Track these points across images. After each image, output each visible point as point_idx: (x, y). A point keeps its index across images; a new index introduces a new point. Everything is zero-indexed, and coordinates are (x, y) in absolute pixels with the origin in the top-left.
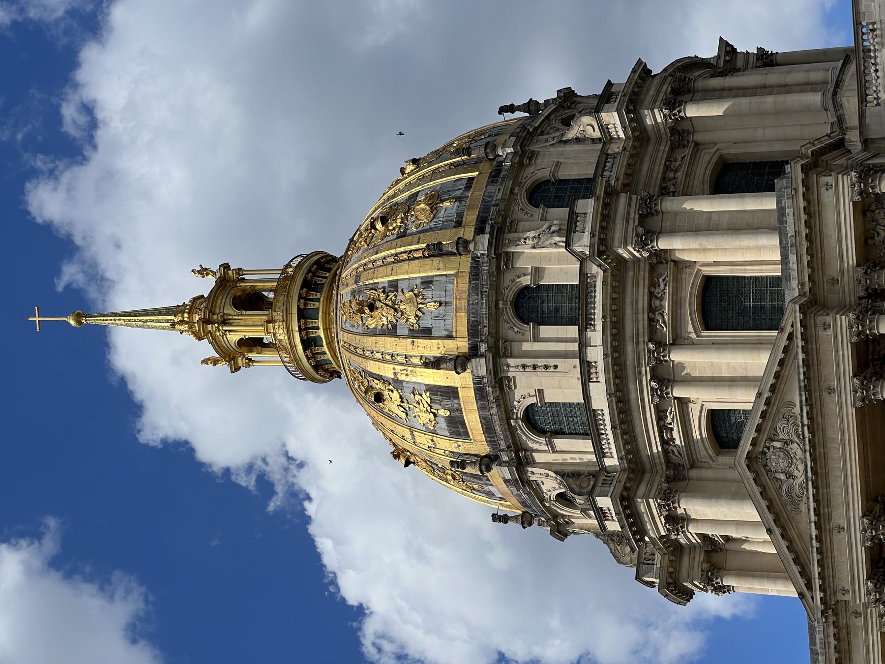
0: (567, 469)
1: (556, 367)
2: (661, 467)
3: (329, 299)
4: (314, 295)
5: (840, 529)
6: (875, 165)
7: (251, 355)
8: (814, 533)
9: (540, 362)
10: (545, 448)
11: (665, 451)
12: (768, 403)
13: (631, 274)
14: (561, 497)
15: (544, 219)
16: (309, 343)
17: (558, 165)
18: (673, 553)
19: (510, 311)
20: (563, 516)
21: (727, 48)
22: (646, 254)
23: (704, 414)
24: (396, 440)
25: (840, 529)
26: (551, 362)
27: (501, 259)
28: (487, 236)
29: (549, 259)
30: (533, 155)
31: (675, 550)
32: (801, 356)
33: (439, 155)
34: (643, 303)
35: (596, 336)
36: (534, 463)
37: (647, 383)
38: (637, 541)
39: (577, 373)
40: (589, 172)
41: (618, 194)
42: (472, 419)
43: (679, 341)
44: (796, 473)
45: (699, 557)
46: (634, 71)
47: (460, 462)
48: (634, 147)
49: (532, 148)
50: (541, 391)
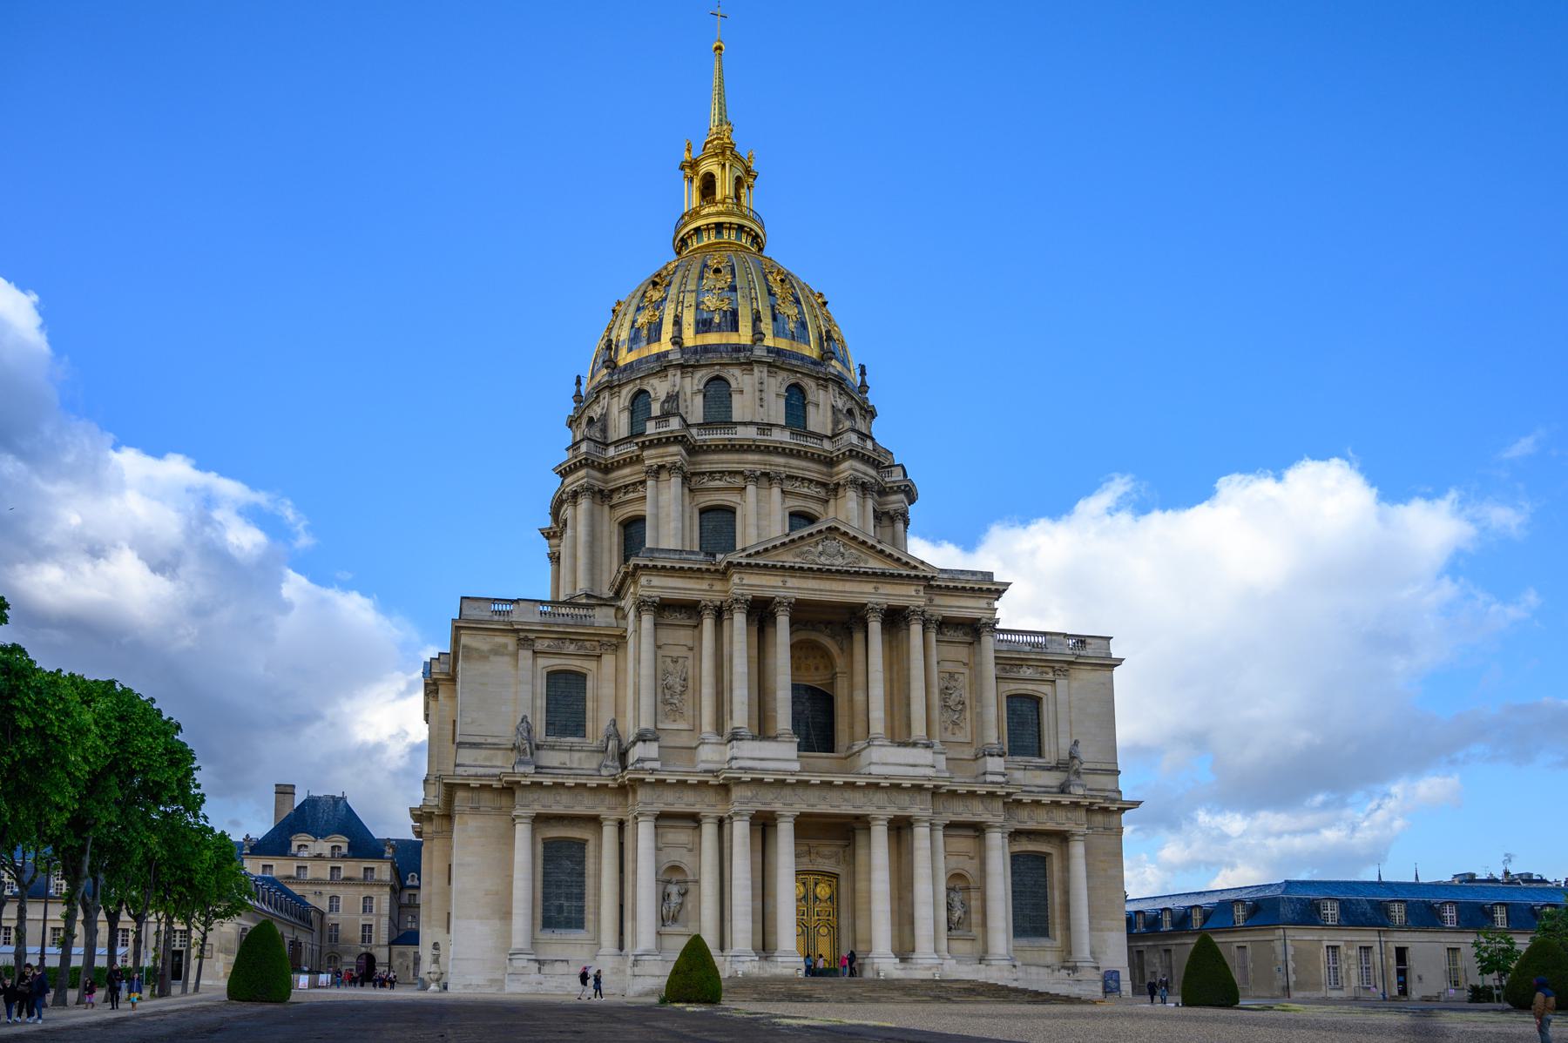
2: (692, 469)
5: (784, 582)
7: (696, 182)
13: (825, 470)
14: (642, 392)
16: (719, 227)
24: (677, 280)
25: (784, 582)
27: (825, 381)
34: (808, 475)
37: (760, 469)
42: (712, 339)
47: (677, 322)
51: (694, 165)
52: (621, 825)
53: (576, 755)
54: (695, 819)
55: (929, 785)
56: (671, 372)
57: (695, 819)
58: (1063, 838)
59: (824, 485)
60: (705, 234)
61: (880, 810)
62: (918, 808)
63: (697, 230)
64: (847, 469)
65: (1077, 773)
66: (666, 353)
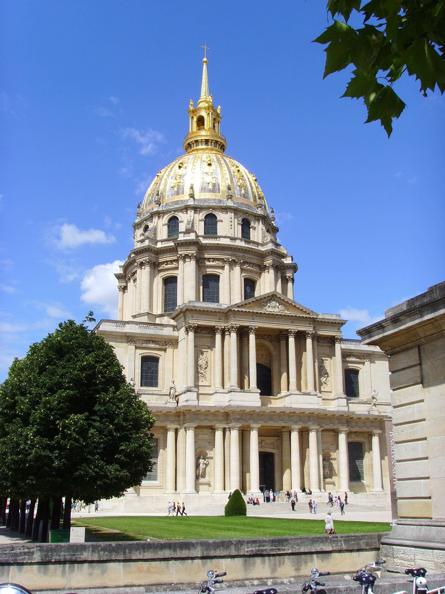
1: (231, 228)
4: (220, 147)
8: (255, 311)
9: (233, 224)
10: (201, 218)
16: (207, 142)
18: (157, 252)
19: (245, 217)
20: (163, 216)
22: (267, 265)
23: (218, 274)
26: (233, 227)
27: (258, 218)
29: (258, 232)
32: (305, 316)
36: (195, 213)
38: (178, 244)
43: (242, 270)
44: (270, 309)
45: (154, 260)
47: (192, 188)
50: (222, 221)
52: (176, 431)
53: (155, 397)
54: (213, 429)
63: (197, 141)
65: (375, 405)
66: (187, 201)
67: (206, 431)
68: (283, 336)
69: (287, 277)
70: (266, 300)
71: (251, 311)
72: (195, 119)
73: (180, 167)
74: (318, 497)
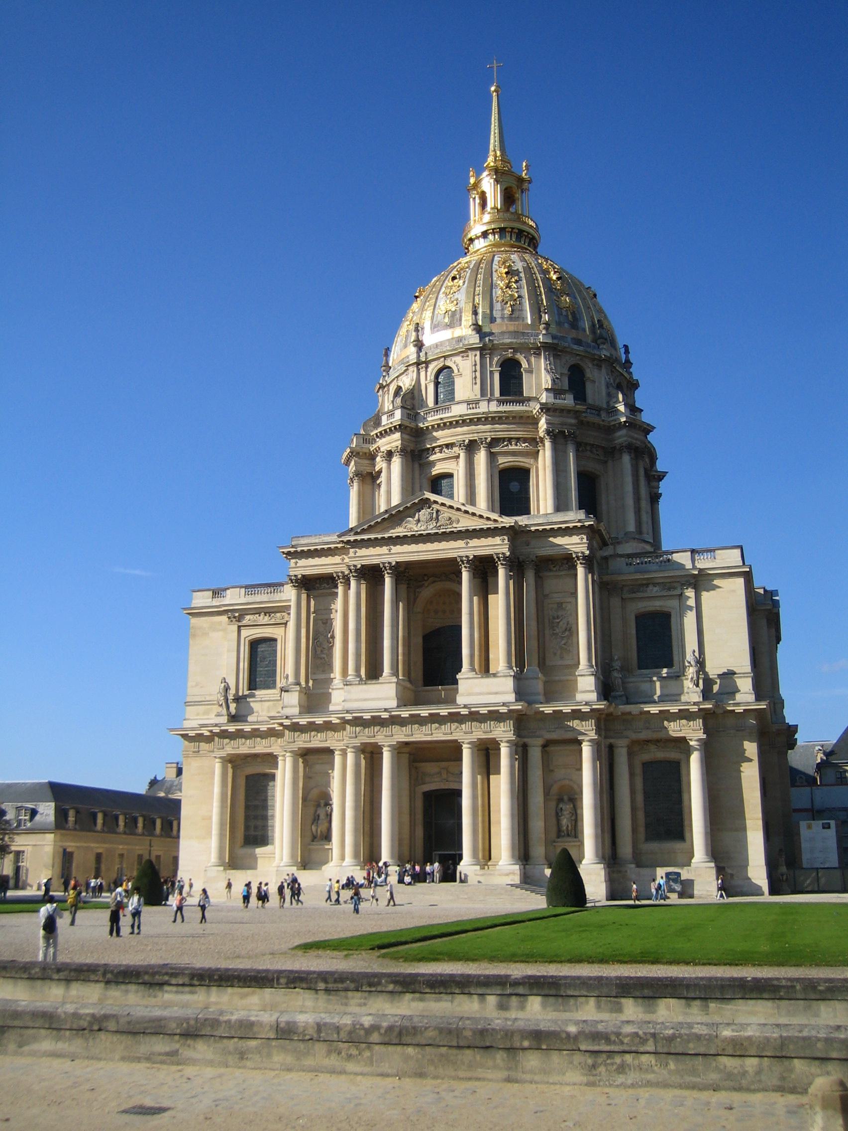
0: (416, 393)
3: (513, 246)
6: (593, 564)
8: (386, 536)
9: (478, 374)
11: (429, 449)
12: (458, 509)
14: (399, 388)
15: (561, 374)
16: (485, 235)
17: (594, 382)
21: (661, 476)
23: (450, 471)
26: (478, 381)
27: (537, 350)
28: (550, 341)
30: (599, 367)
31: (372, 457)
32: (485, 527)
33: (600, 311)
34: (513, 434)
35: (494, 407)
37: (467, 438)
39: (473, 397)
40: (590, 400)
41: (576, 418)
45: (369, 470)
46: (648, 425)
48: (604, 426)
49: (603, 366)
51: (476, 185)
53: (267, 704)
55: (503, 710)
56: (411, 369)
57: (329, 752)
58: (682, 743)
59: (534, 439)
60: (476, 241)
61: (466, 736)
62: (503, 733)
64: (543, 424)
67: (325, 757)
68: (448, 570)
69: (618, 447)
70: (412, 511)
71: (379, 536)
72: (477, 201)
73: (417, 297)
74: (507, 875)
